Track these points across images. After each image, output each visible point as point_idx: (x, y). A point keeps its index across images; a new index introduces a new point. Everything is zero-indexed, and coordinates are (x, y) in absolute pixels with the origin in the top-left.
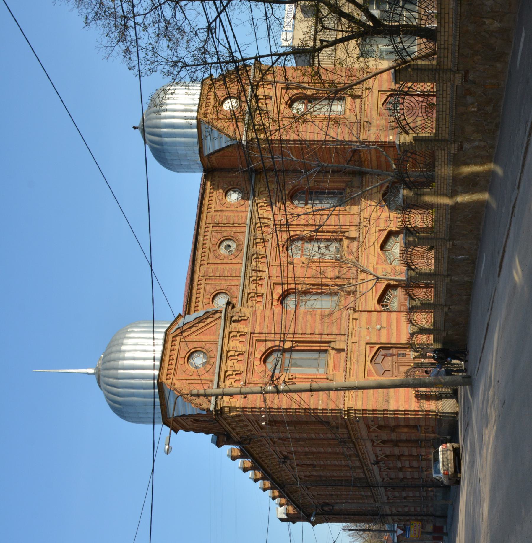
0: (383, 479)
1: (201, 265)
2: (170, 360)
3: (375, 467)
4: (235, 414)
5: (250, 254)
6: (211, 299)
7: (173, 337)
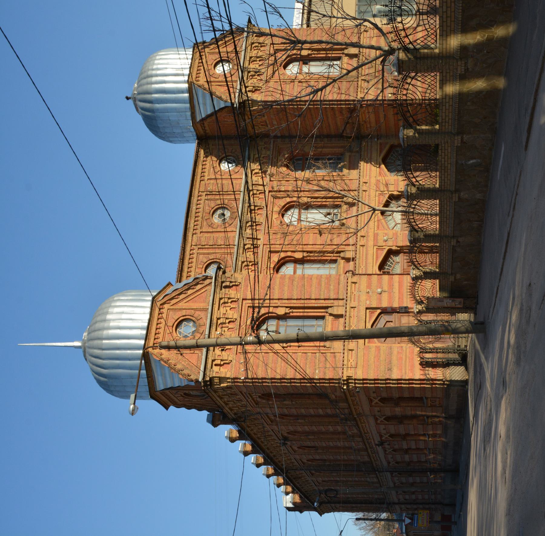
0: (389, 463)
1: (193, 234)
2: (157, 329)
3: (380, 449)
4: (225, 385)
5: (245, 222)
6: (203, 269)
7: (161, 305)
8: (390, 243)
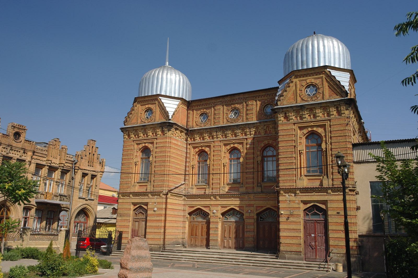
8: (212, 214)
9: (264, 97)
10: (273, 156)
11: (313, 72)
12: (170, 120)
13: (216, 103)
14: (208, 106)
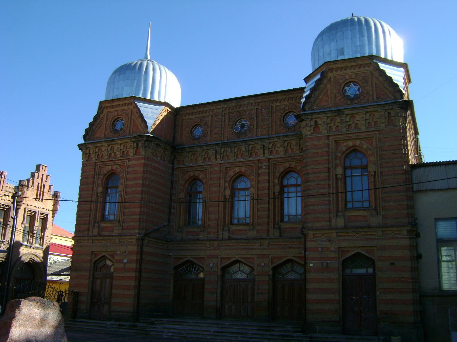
6: (197, 123)
9: (284, 101)
10: (296, 185)
11: (354, 64)
12: (148, 133)
13: (215, 111)
14: (204, 115)
